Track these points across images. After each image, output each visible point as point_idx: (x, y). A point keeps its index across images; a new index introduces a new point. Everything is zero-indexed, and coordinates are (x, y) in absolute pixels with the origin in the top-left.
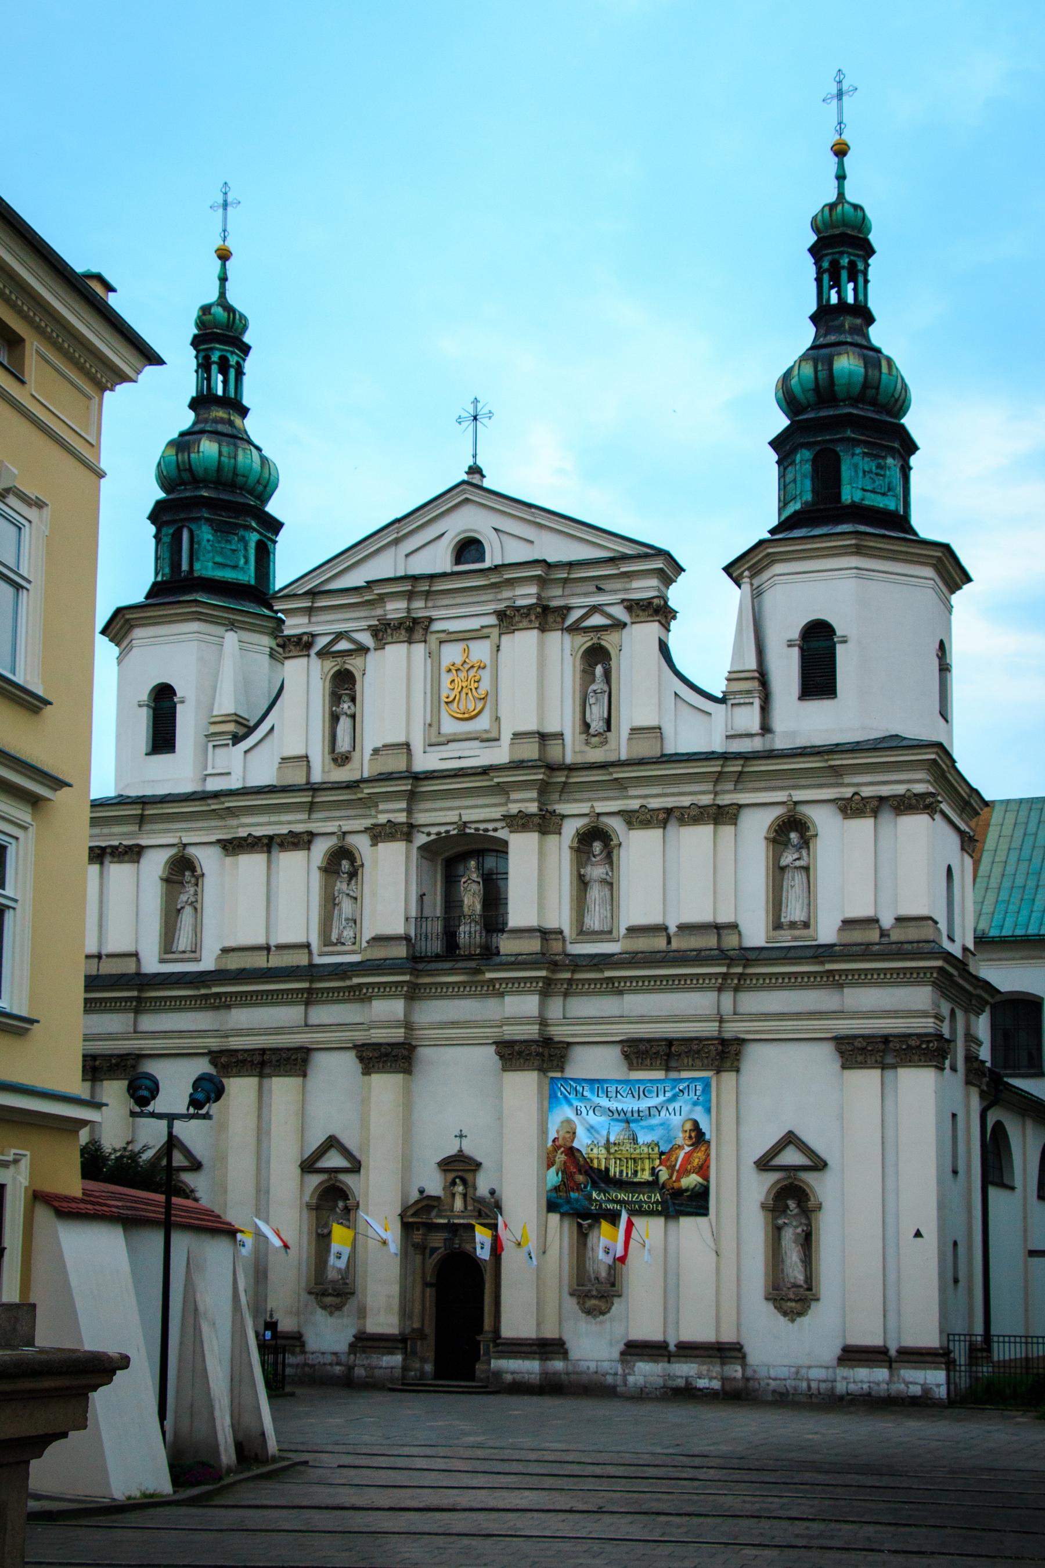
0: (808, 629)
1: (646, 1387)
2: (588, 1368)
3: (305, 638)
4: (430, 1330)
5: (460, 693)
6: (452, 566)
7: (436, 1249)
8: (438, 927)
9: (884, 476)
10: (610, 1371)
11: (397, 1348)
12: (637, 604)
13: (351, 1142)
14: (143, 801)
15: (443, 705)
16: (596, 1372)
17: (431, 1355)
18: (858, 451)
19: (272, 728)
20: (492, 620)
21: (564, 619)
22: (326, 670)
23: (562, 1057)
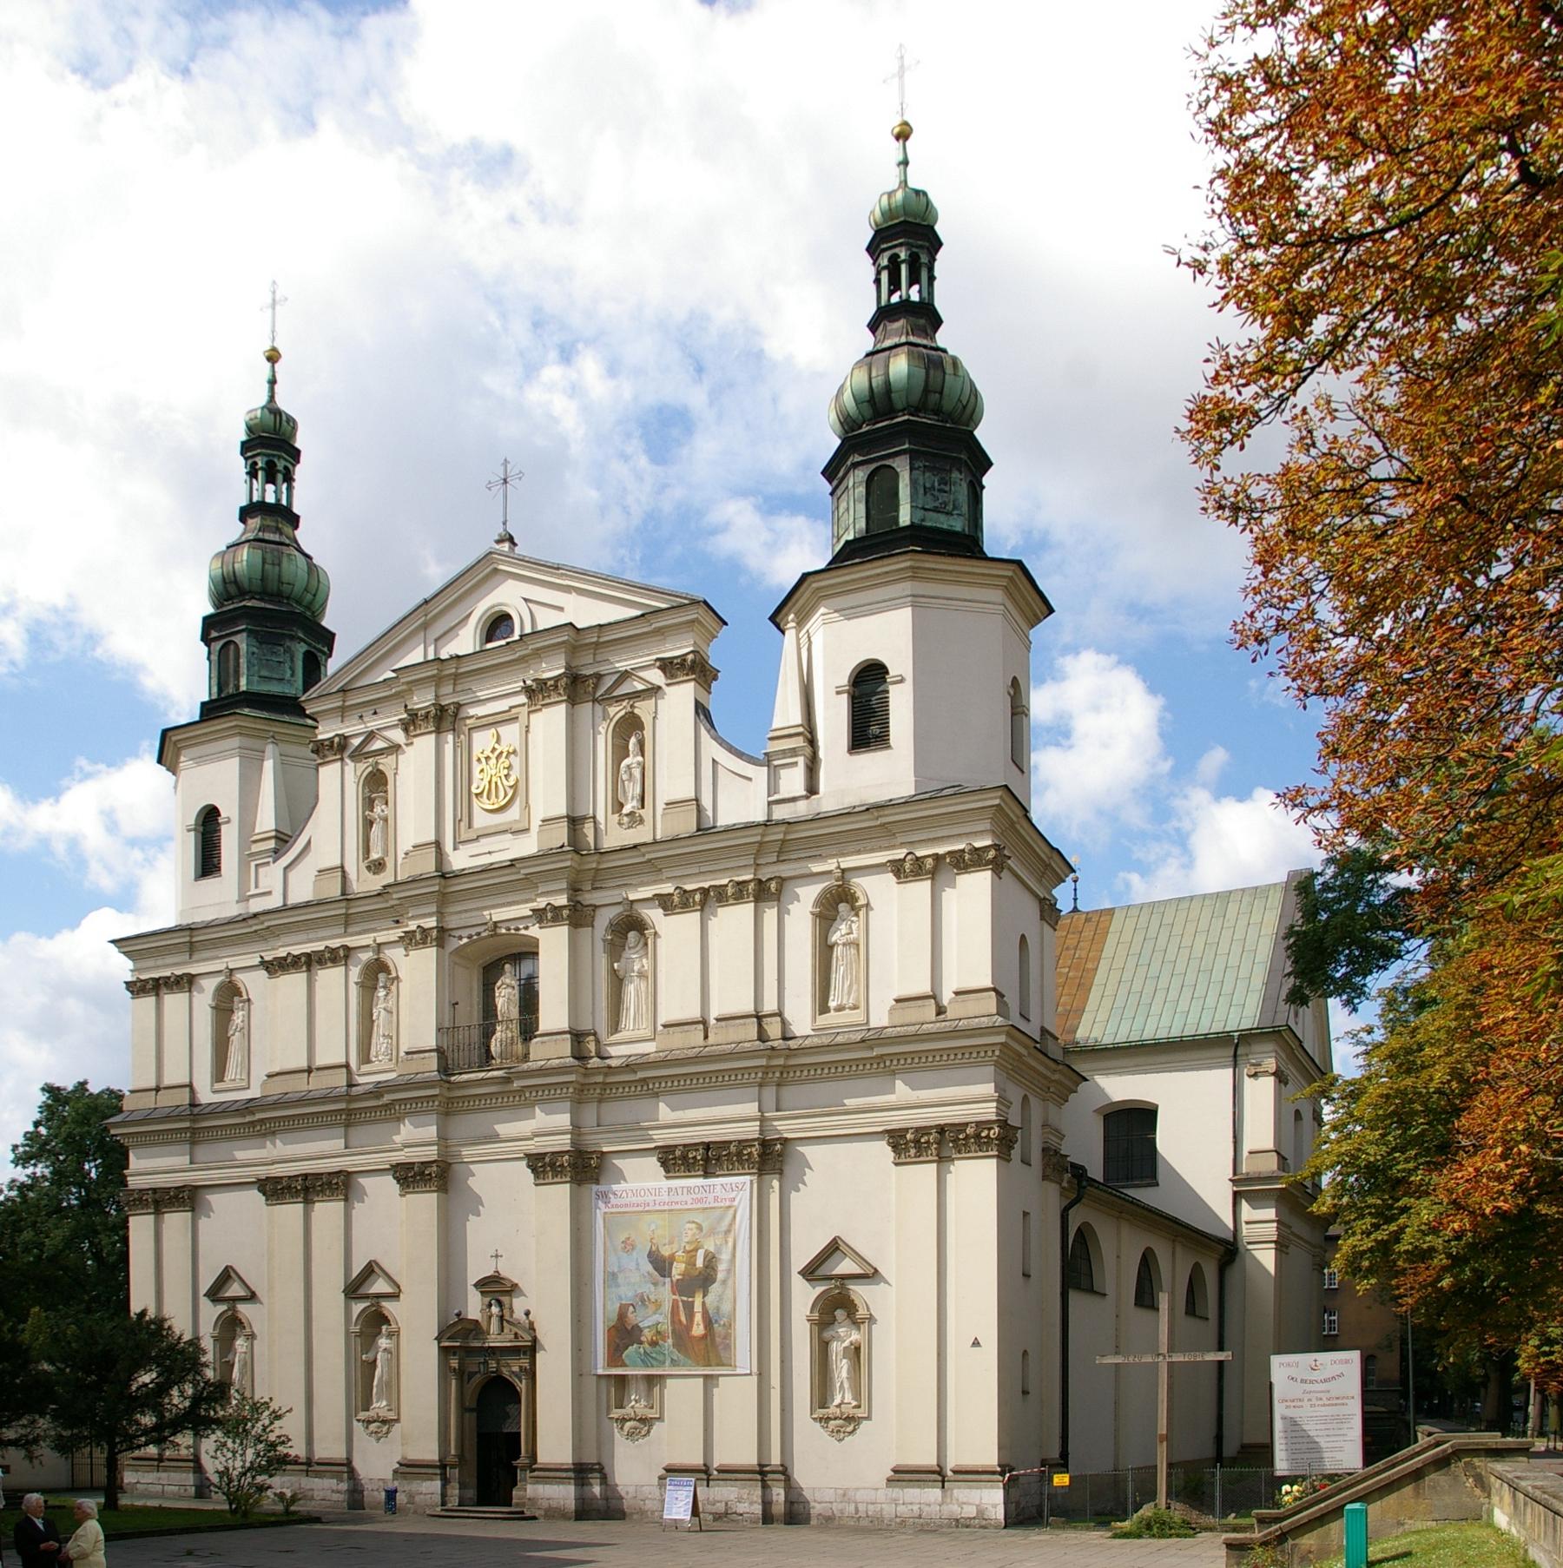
0: (856, 677)
3: (337, 740)
5: (490, 782)
6: (481, 645)
8: (476, 1035)
14: (190, 929)
19: (309, 842)
20: (522, 699)
21: (596, 687)
22: (359, 774)
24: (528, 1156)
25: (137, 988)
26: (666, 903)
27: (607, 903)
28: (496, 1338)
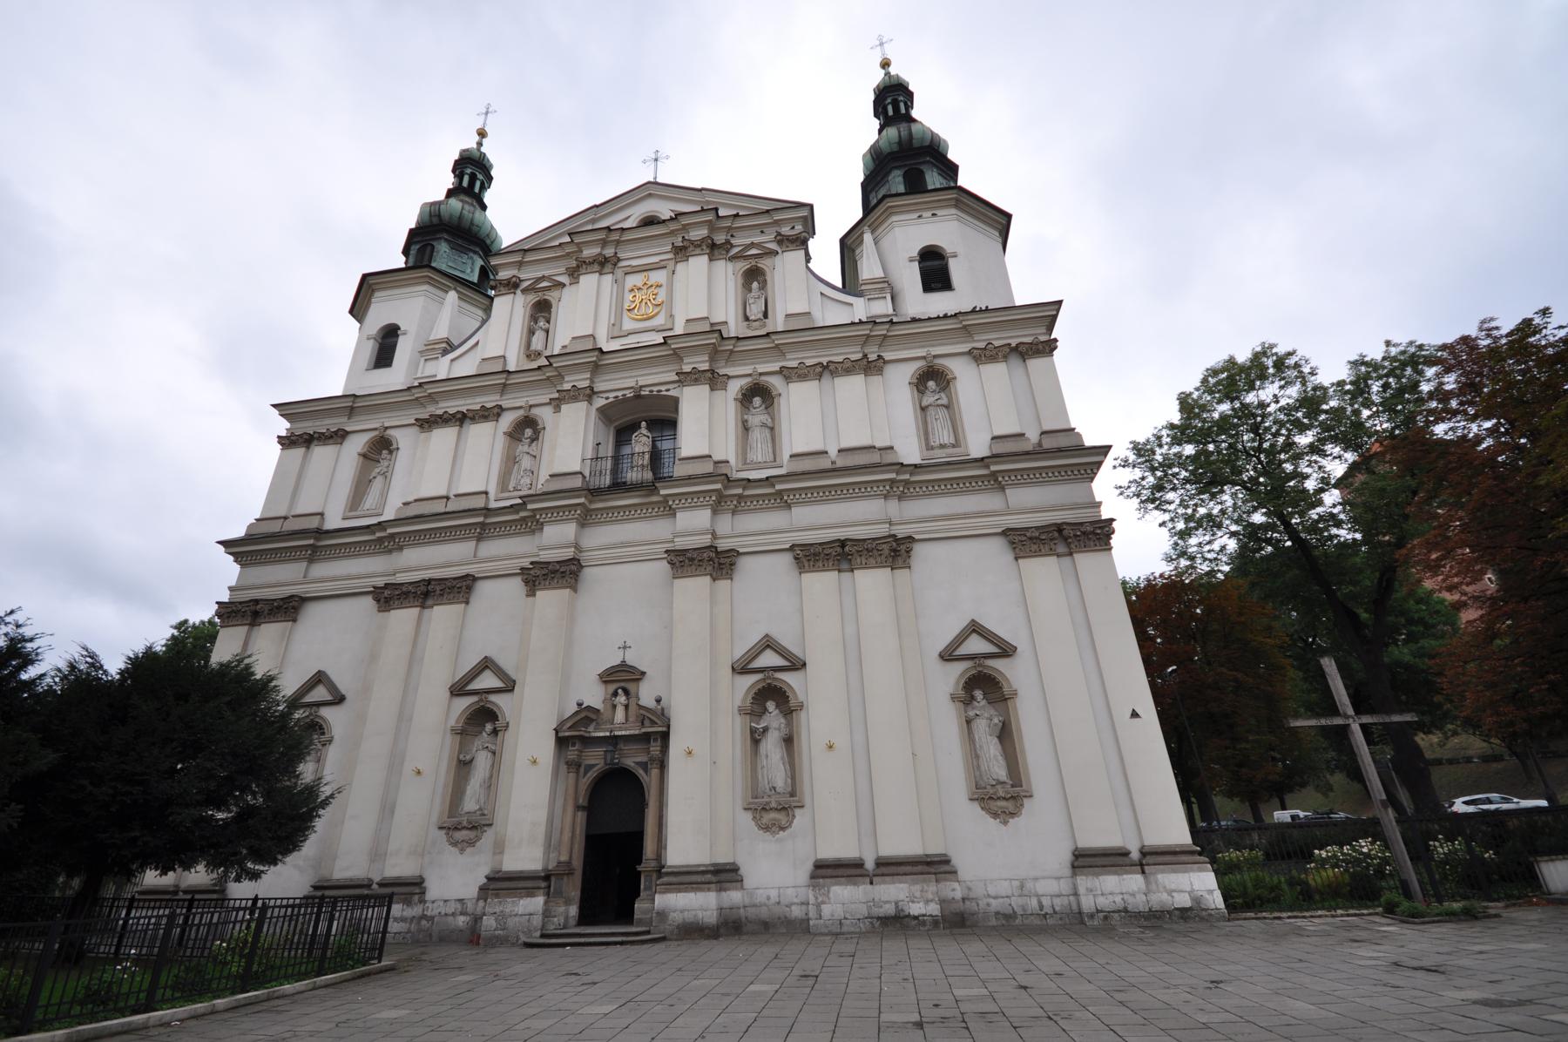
1: (846, 918)
2: (768, 898)
4: (578, 863)
7: (592, 766)
10: (796, 900)
11: (539, 888)
12: (787, 239)
13: (507, 662)
14: (354, 396)
15: (625, 312)
16: (779, 903)
17: (575, 894)
19: (477, 343)
21: (728, 252)
23: (731, 565)
25: (287, 442)
26: (787, 374)
27: (739, 375)
28: (620, 721)
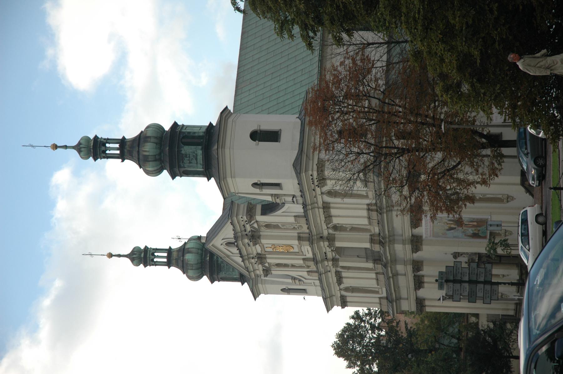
9: (189, 155)
18: (182, 165)
24: (412, 253)
